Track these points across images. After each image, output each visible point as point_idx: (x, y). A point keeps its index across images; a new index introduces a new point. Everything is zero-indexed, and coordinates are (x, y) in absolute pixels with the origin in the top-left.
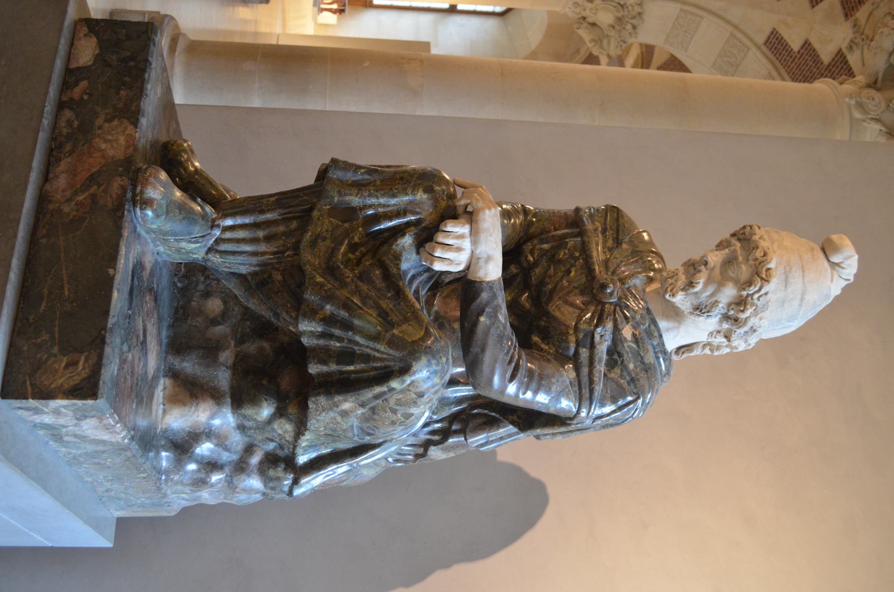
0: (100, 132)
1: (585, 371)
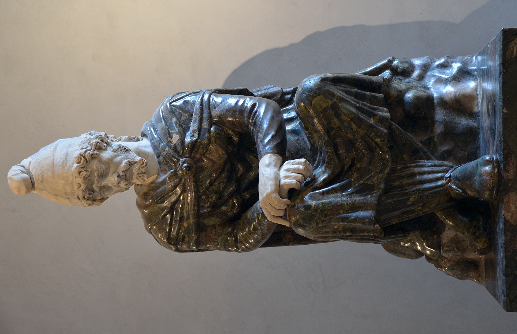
1: (205, 115)
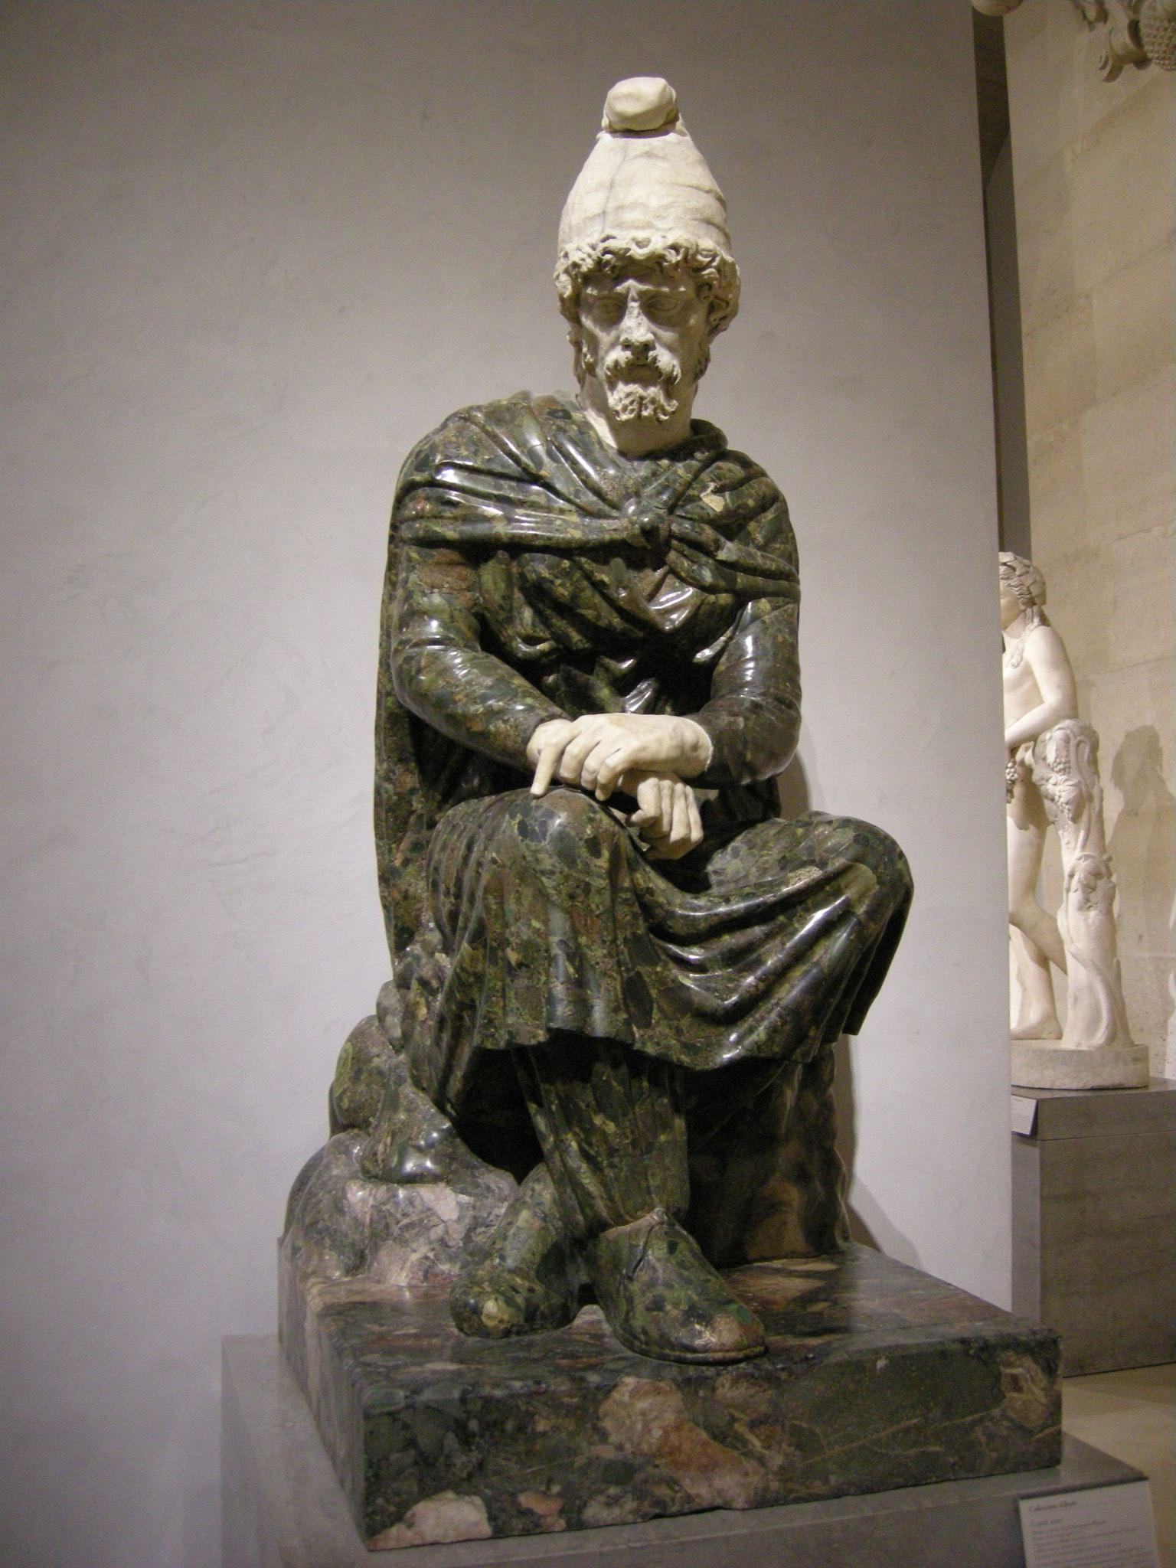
0: (628, 1446)
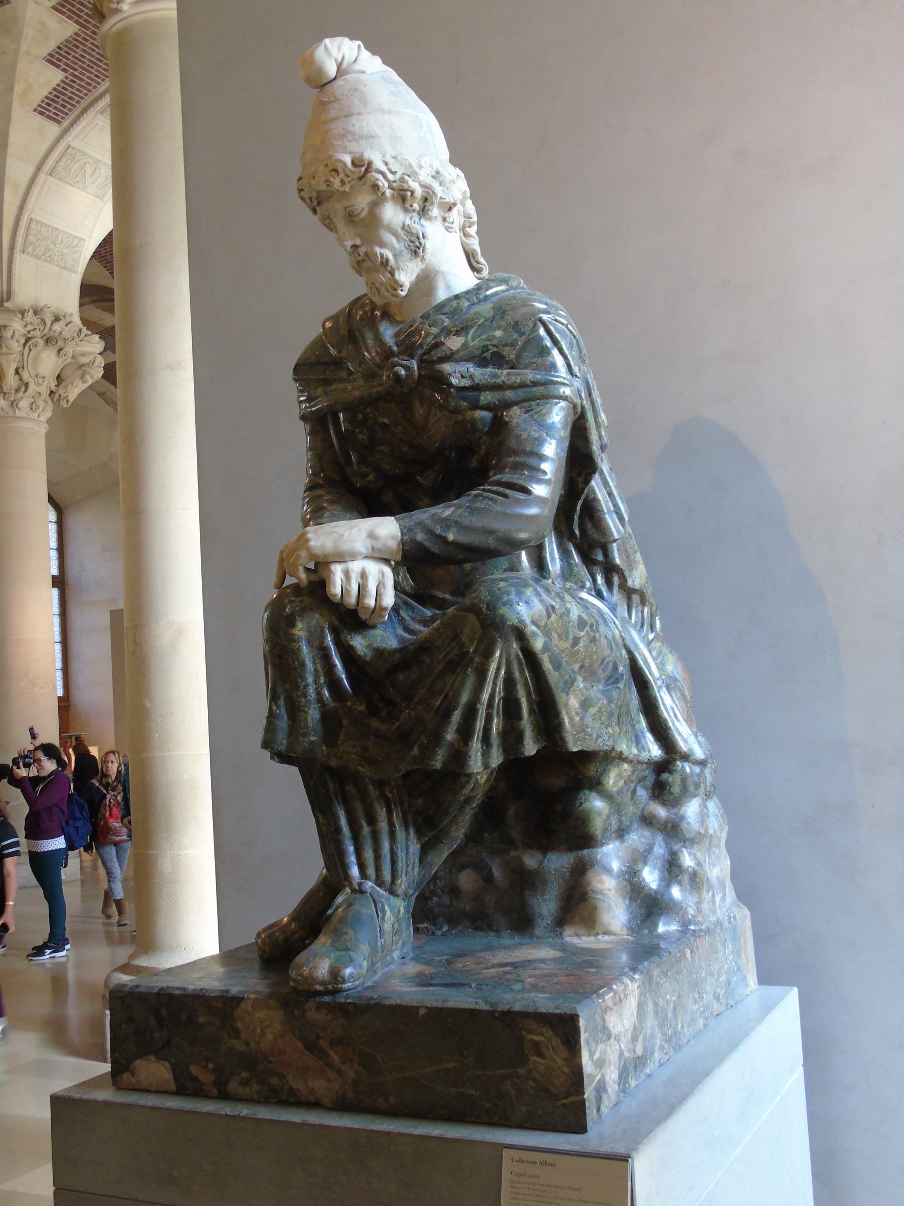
0: (252, 1043)
1: (509, 394)
